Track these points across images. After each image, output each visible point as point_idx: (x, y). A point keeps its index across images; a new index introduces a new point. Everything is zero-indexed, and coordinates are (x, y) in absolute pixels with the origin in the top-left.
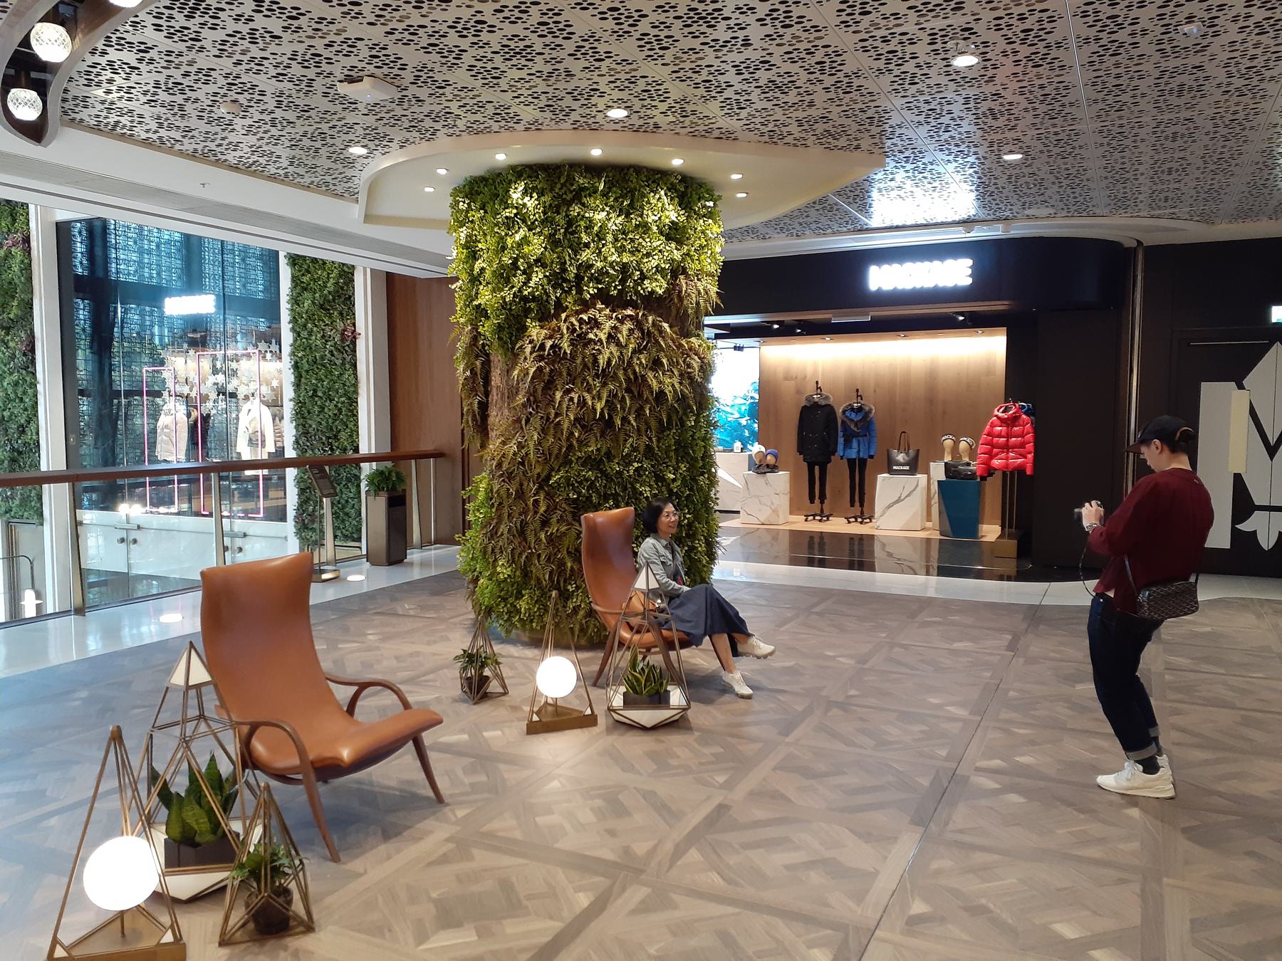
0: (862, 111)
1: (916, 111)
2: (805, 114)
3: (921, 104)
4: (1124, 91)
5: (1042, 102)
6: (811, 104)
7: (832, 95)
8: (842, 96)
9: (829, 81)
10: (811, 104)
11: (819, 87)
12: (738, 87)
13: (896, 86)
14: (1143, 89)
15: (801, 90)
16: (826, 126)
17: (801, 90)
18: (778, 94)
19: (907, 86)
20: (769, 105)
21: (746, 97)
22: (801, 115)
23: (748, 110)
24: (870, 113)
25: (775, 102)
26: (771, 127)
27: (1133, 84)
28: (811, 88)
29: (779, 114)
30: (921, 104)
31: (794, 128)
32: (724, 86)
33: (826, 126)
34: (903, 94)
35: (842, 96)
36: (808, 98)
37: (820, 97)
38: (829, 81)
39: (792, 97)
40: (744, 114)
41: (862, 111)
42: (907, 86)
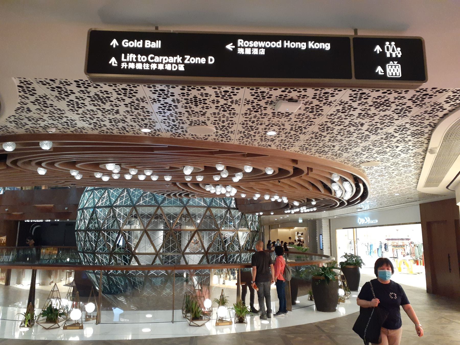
0: (142, 120)
1: (167, 124)
2: (113, 117)
3: (171, 122)
4: (252, 130)
5: (221, 129)
6: (117, 112)
7: (129, 109)
8: (133, 110)
9: (128, 101)
10: (117, 112)
11: (122, 103)
12: (78, 95)
13: (161, 110)
14: (260, 130)
15: (113, 103)
16: (123, 125)
17: (113, 103)
18: (100, 103)
19: (166, 111)
20: (94, 108)
21: (82, 101)
22: (111, 117)
23: (83, 109)
24: (146, 122)
25: (98, 107)
26: (95, 120)
27: (257, 127)
28: (118, 102)
29: (100, 114)
30: (171, 122)
31: (107, 123)
32: (69, 92)
33: (123, 125)
34: (163, 115)
35: (133, 110)
36: (116, 108)
37: (122, 109)
38: (128, 101)
39: (107, 106)
40: (80, 111)
41: (142, 120)
42: (166, 111)
